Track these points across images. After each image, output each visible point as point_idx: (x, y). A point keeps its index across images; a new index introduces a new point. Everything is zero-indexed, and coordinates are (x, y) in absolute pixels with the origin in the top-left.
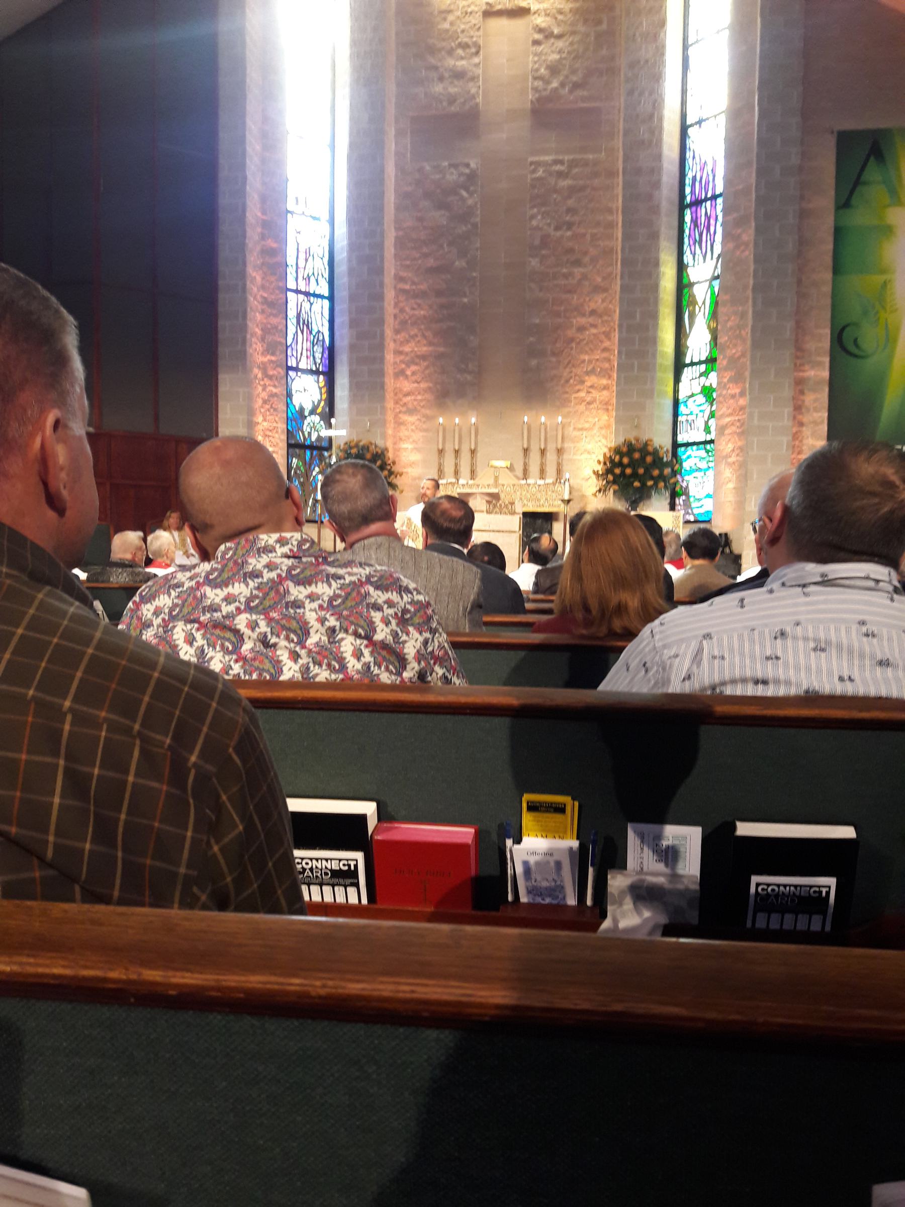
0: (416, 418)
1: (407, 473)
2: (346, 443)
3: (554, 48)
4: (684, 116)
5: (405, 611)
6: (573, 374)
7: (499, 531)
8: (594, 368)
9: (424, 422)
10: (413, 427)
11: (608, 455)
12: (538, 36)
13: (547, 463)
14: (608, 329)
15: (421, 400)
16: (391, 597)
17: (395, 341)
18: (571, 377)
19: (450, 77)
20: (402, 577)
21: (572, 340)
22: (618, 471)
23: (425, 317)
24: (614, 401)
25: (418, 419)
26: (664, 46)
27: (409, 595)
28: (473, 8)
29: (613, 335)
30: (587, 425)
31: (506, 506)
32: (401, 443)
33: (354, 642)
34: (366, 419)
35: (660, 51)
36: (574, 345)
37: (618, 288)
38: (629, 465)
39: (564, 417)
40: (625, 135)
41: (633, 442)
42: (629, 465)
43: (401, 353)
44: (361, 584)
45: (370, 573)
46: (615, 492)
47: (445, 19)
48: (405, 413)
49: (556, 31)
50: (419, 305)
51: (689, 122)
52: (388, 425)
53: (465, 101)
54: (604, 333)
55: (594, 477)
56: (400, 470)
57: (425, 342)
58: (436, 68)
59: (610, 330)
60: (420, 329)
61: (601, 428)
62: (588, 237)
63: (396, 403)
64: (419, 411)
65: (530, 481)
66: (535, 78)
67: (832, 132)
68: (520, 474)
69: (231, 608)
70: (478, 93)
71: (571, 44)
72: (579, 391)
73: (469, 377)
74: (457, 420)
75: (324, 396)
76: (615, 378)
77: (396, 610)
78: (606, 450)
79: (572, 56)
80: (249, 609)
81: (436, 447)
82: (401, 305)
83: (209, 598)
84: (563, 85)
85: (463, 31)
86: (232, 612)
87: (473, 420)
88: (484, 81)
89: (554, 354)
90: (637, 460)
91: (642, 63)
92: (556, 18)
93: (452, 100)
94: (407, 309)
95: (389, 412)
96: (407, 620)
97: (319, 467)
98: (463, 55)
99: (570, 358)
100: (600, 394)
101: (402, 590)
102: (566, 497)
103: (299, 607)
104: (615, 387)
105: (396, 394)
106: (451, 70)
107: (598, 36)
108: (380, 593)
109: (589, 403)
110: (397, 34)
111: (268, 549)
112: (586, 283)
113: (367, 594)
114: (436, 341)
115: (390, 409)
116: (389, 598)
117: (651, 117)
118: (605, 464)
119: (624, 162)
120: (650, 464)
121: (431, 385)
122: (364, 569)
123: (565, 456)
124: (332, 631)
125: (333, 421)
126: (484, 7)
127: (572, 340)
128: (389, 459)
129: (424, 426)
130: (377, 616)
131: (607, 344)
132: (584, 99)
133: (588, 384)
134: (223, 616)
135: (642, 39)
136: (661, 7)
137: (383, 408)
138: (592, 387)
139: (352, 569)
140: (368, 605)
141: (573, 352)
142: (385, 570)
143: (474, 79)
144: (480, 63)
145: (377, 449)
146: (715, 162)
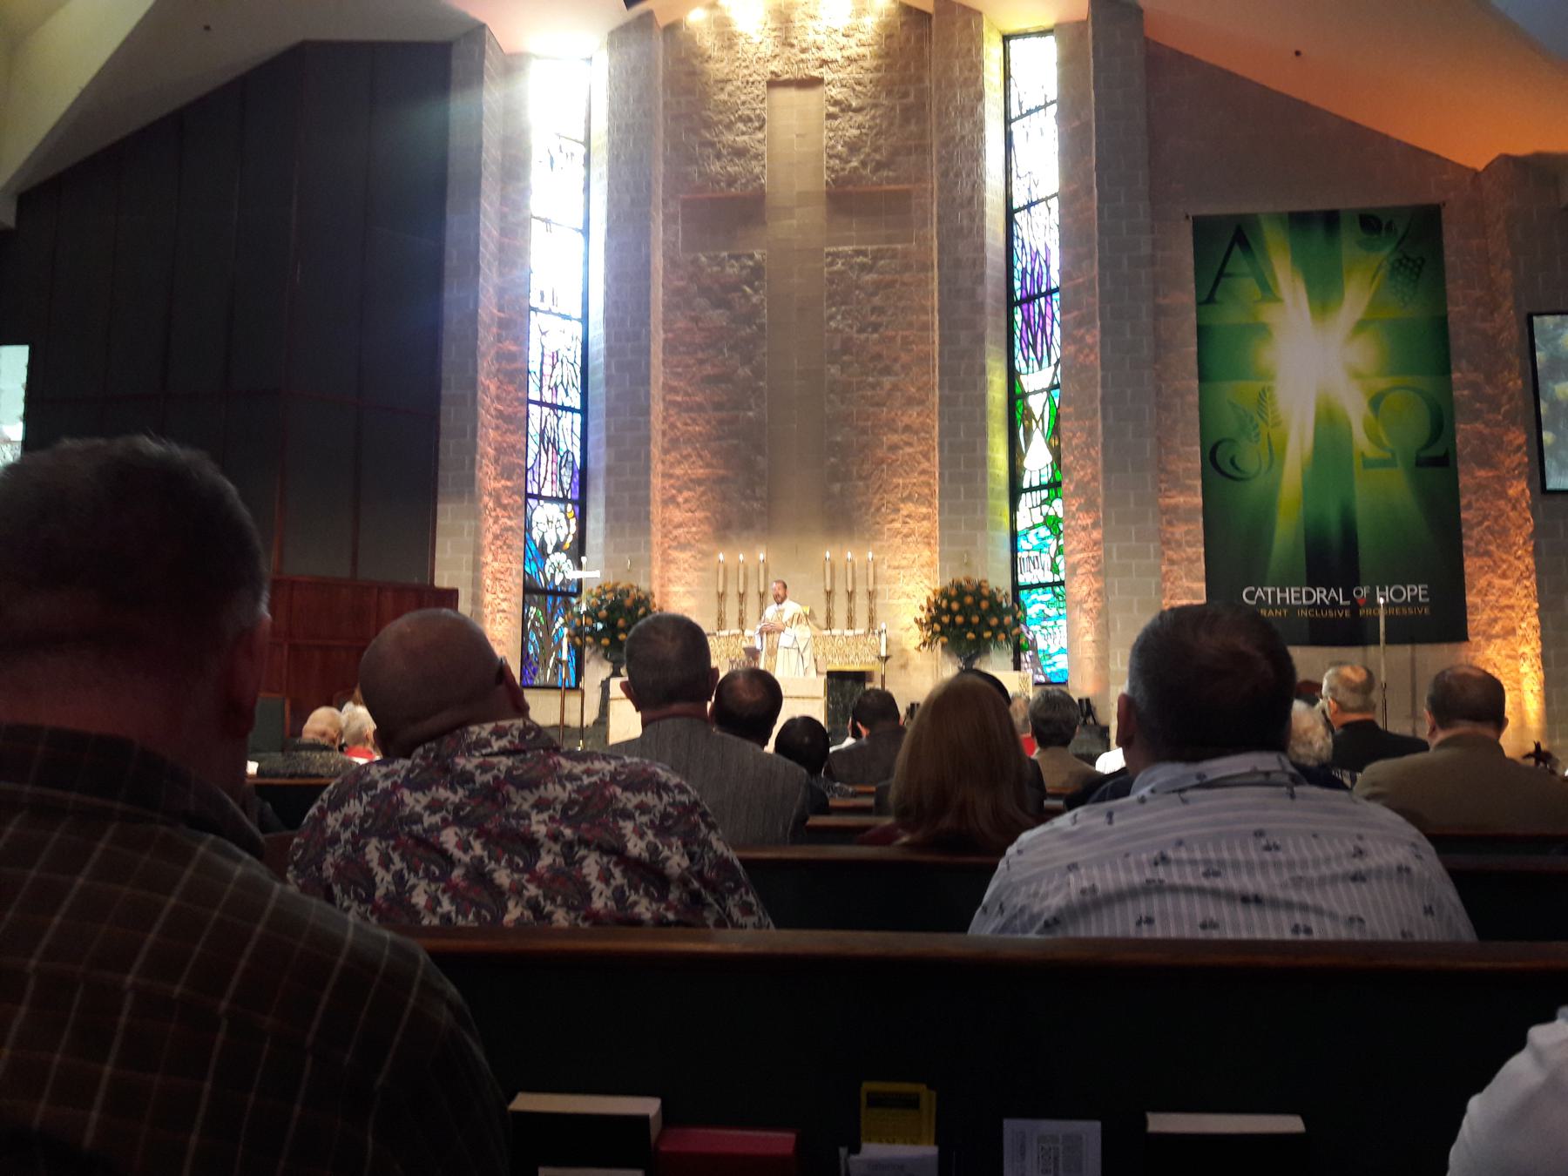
0: (689, 554)
2: (600, 587)
3: (852, 123)
4: (1009, 199)
5: (665, 816)
7: (798, 697)
9: (700, 560)
11: (933, 599)
12: (832, 109)
14: (926, 448)
15: (696, 533)
16: (645, 799)
17: (663, 462)
19: (729, 154)
20: (659, 770)
21: (882, 461)
22: (946, 619)
23: (700, 434)
25: (692, 556)
26: (982, 121)
27: (670, 794)
28: (755, 77)
29: (932, 455)
30: (904, 563)
32: (671, 586)
33: (599, 860)
35: (979, 127)
36: (885, 466)
37: (937, 400)
38: (959, 612)
39: (875, 552)
41: (964, 583)
42: (959, 612)
43: (671, 476)
44: (604, 784)
45: (616, 769)
47: (722, 89)
48: (676, 548)
49: (854, 104)
51: (1015, 206)
53: (748, 181)
54: (921, 453)
55: (916, 627)
57: (701, 463)
58: (712, 144)
59: (929, 450)
60: (695, 449)
61: (922, 566)
62: (899, 339)
63: (665, 536)
64: (693, 546)
65: (834, 632)
66: (830, 157)
68: (823, 623)
69: (437, 818)
70: (762, 173)
71: (873, 118)
74: (741, 557)
75: (573, 529)
76: (937, 506)
77: (652, 816)
78: (930, 593)
79: (874, 131)
80: (459, 821)
82: (672, 419)
83: (408, 805)
84: (864, 164)
85: (744, 103)
86: (437, 823)
87: (762, 557)
89: (860, 478)
90: (969, 606)
92: (854, 90)
93: (732, 181)
94: (679, 425)
96: (669, 828)
97: (563, 617)
98: (744, 129)
99: (880, 482)
100: (919, 524)
101: (661, 788)
102: (883, 654)
103: (523, 818)
104: (937, 517)
105: (664, 526)
106: (729, 146)
107: (906, 110)
108: (629, 795)
109: (907, 536)
110: (665, 104)
111: (485, 743)
112: (899, 394)
113: (614, 796)
114: (714, 462)
115: (657, 543)
116: (642, 801)
117: (971, 200)
118: (929, 610)
119: (940, 252)
120: (986, 611)
121: (708, 514)
122: (609, 763)
123: (879, 601)
124: (569, 847)
125: (584, 559)
126: (769, 76)
127: (882, 461)
128: (655, 606)
129: (701, 565)
130: (628, 827)
131: (925, 465)
132: (889, 180)
133: (904, 512)
134: (424, 830)
135: (956, 113)
137: (648, 544)
138: (909, 516)
139: (592, 763)
140: (615, 811)
142: (636, 763)
143: (757, 156)
145: (640, 594)
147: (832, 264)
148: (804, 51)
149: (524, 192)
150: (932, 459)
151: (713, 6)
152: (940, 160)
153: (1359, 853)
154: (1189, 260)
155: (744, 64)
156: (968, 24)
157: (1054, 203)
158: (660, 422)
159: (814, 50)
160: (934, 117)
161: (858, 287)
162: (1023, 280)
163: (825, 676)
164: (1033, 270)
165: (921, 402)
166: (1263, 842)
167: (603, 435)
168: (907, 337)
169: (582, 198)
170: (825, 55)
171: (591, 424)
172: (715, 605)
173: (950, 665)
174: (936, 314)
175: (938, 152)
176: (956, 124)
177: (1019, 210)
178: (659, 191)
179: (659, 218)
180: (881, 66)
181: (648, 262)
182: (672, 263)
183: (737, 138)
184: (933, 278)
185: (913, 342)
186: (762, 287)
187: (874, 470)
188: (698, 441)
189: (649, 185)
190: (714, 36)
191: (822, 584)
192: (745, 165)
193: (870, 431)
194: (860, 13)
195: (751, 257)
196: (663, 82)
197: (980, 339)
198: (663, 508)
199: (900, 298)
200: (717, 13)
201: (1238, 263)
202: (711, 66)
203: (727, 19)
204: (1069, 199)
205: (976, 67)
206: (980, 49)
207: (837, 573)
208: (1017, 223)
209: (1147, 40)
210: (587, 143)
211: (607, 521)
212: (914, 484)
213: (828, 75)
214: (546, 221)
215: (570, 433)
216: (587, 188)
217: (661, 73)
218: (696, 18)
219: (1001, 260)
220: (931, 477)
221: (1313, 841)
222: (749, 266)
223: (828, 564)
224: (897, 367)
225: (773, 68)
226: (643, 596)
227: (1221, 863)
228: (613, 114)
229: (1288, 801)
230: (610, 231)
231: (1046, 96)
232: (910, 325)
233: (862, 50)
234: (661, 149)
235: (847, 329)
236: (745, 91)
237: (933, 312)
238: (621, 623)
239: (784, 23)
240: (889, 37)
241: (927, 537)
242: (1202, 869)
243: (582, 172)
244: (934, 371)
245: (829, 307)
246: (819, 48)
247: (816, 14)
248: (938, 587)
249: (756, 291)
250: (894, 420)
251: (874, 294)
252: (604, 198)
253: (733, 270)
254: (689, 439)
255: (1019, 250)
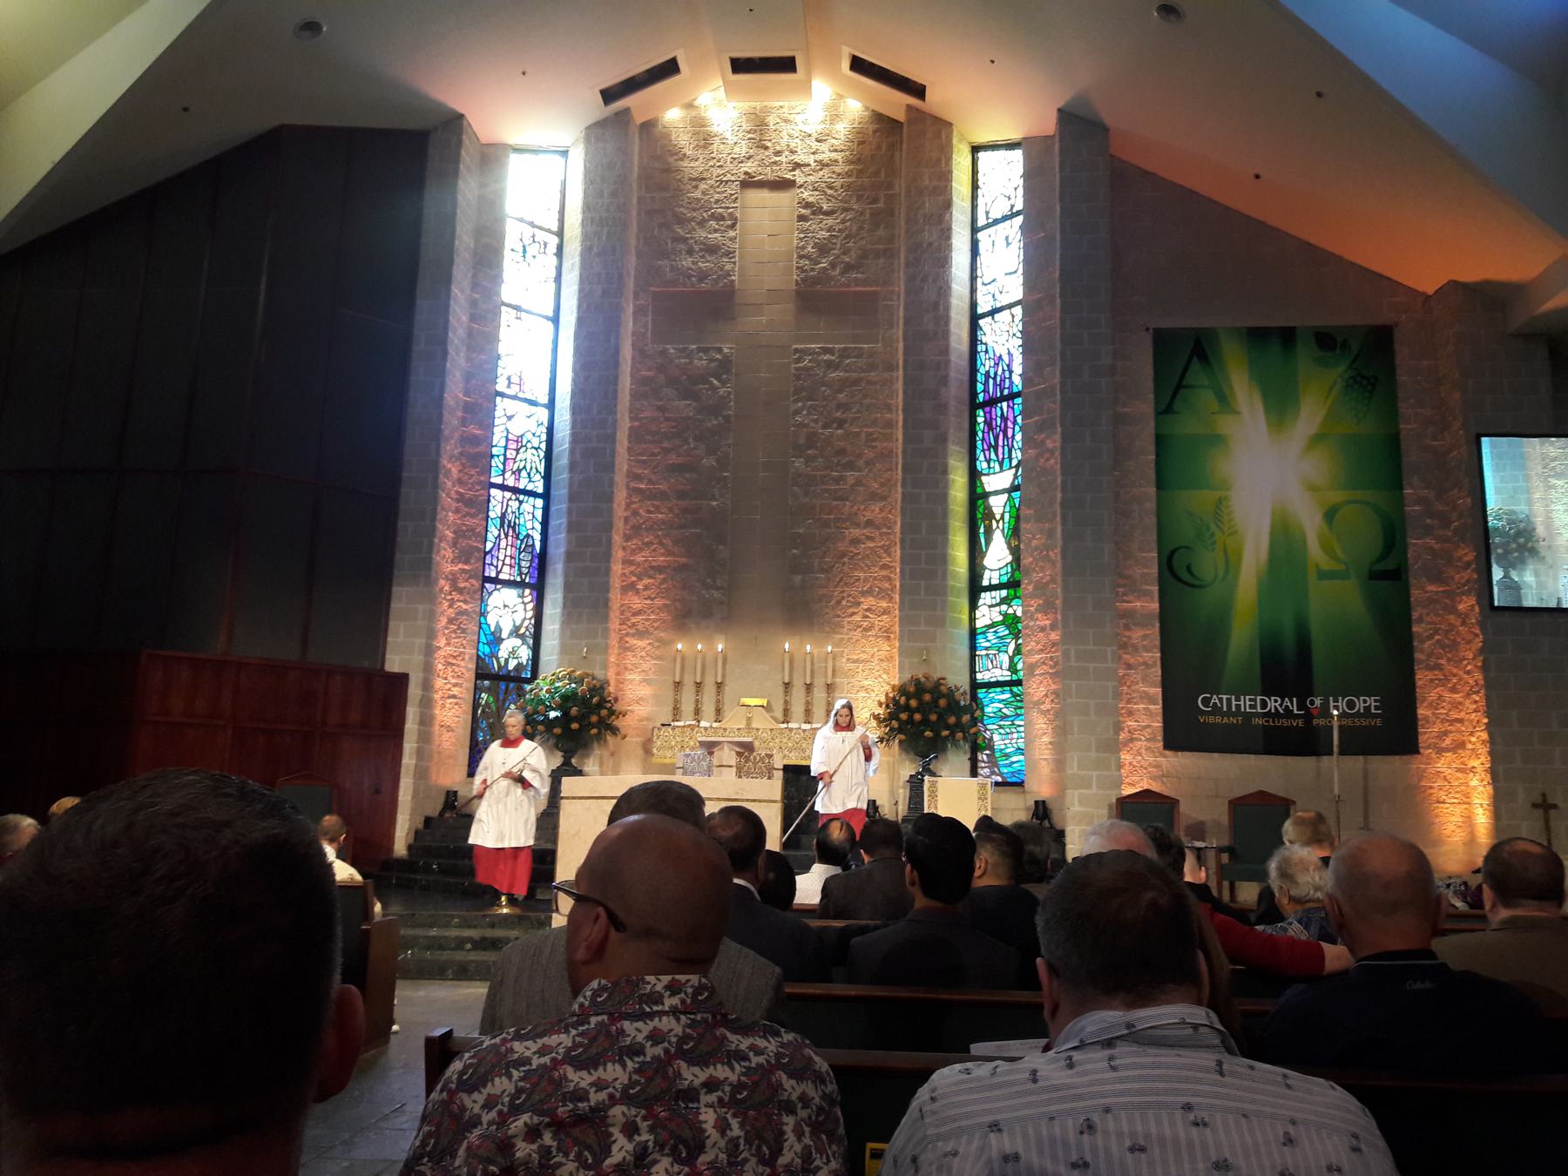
1: (632, 711)
4: (973, 305)
6: (845, 595)
8: (870, 588)
10: (643, 654)
11: (891, 695)
12: (803, 211)
13: (815, 702)
14: (887, 543)
15: (655, 621)
17: (624, 549)
18: (843, 598)
19: (701, 250)
21: (844, 555)
22: (904, 716)
23: (663, 522)
24: (897, 628)
25: (650, 644)
26: (950, 229)
29: (893, 549)
30: (863, 656)
31: (762, 759)
32: (627, 673)
34: (583, 643)
35: (946, 234)
36: (846, 560)
37: (899, 497)
38: (917, 710)
40: (905, 324)
41: (923, 680)
42: (917, 710)
43: (631, 563)
46: (900, 742)
47: (696, 187)
48: (633, 635)
49: (825, 207)
50: (657, 508)
51: (980, 311)
52: (610, 651)
53: (719, 277)
54: (882, 547)
55: (874, 723)
56: (624, 708)
57: (662, 551)
61: (882, 660)
62: (863, 435)
64: (652, 633)
65: (791, 725)
66: (801, 257)
67: (1147, 329)
68: (779, 714)
71: (843, 221)
72: (853, 614)
73: (716, 594)
74: (699, 647)
75: (530, 614)
76: (898, 600)
78: (888, 688)
81: (670, 680)
82: (634, 506)
84: (833, 265)
85: (717, 201)
87: (720, 647)
88: (741, 257)
89: (822, 570)
90: (928, 703)
91: (925, 245)
92: (826, 194)
93: (703, 276)
95: (613, 635)
104: (897, 612)
105: (622, 613)
106: (702, 243)
107: (874, 214)
109: (867, 630)
110: (640, 199)
112: (861, 489)
114: (676, 549)
117: (936, 305)
118: (887, 706)
119: (905, 354)
127: (844, 555)
131: (887, 560)
132: (857, 282)
136: (946, 187)
137: (606, 630)
138: (867, 610)
141: (846, 568)
143: (729, 254)
144: (735, 238)
146: (1009, 353)
147: (798, 360)
148: (778, 153)
149: (497, 279)
150: (893, 554)
151: (690, 106)
152: (907, 265)
153: (1289, 1141)
154: (1148, 371)
155: (718, 164)
156: (938, 135)
157: (1018, 311)
158: (623, 508)
159: (787, 153)
160: (903, 223)
161: (823, 384)
162: (986, 384)
163: (781, 773)
164: (996, 374)
165: (883, 498)
166: (1191, 1117)
167: (564, 520)
168: (871, 434)
169: (553, 286)
170: (800, 158)
171: (553, 508)
172: (671, 694)
173: (907, 762)
174: (900, 412)
175: (906, 258)
176: (923, 231)
177: (984, 316)
178: (630, 284)
179: (630, 310)
180: (851, 171)
181: (617, 352)
182: (640, 353)
183: (710, 236)
184: (897, 378)
185: (876, 440)
186: (729, 380)
187: (836, 563)
188: (662, 530)
189: (621, 277)
190: (689, 135)
191: (780, 676)
192: (716, 261)
193: (832, 525)
194: (835, 117)
195: (720, 350)
196: (639, 177)
197: (942, 439)
198: (622, 594)
199: (865, 396)
200: (694, 113)
201: (1197, 375)
202: (685, 164)
203: (703, 119)
204: (1032, 305)
205: (945, 177)
206: (949, 159)
207: (795, 666)
208: (981, 329)
209: (1111, 156)
210: (560, 234)
211: (565, 606)
212: (875, 579)
213: (799, 177)
214: (517, 308)
215: (531, 517)
216: (558, 279)
217: (636, 169)
218: (673, 116)
219: (964, 363)
220: (892, 572)
221: (1243, 1120)
222: (717, 360)
223: (787, 655)
224: (861, 463)
225: (746, 169)
226: (598, 686)
227: (1148, 1136)
228: (587, 208)
229: (1219, 1077)
230: (581, 321)
231: (1012, 206)
232: (875, 423)
233: (834, 155)
234: (633, 242)
235: (812, 424)
236: (718, 190)
237: (897, 411)
238: (574, 711)
239: (759, 129)
240: (861, 143)
241: (886, 631)
242: (1128, 1143)
243: (554, 260)
244: (897, 468)
245: (796, 401)
246: (793, 152)
247: (791, 117)
248: (896, 682)
249: (724, 383)
250: (856, 514)
251: (841, 391)
252: (575, 288)
253: (701, 362)
254: (651, 527)
255: (982, 354)
